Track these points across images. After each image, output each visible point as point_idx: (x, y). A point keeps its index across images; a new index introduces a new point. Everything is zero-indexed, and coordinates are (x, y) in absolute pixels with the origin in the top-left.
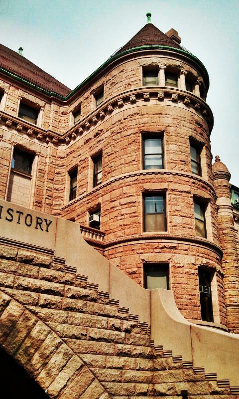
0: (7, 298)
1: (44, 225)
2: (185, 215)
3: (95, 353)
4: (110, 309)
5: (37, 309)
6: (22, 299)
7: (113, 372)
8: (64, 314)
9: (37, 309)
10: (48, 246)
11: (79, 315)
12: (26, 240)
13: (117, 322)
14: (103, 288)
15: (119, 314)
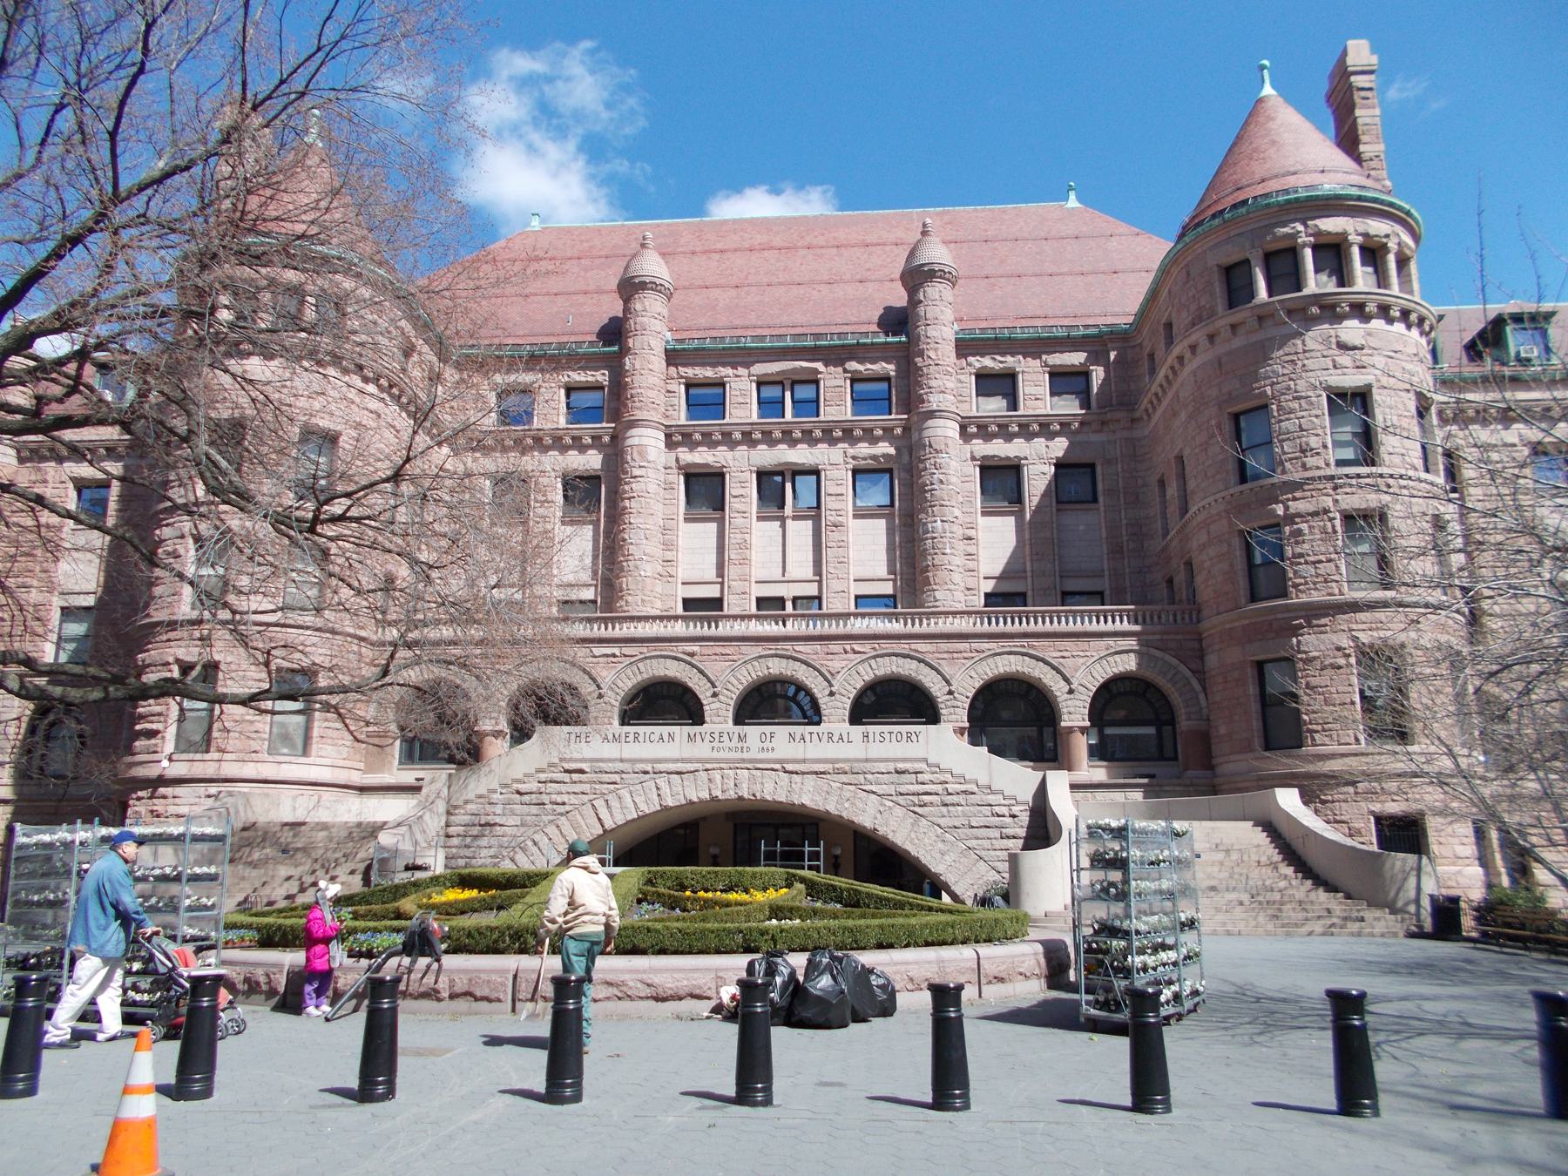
0: (891, 804)
1: (914, 736)
2: (1317, 558)
3: (977, 838)
4: (992, 799)
5: (917, 809)
6: (902, 802)
7: (998, 853)
8: (944, 809)
9: (917, 809)
10: (921, 755)
11: (960, 808)
12: (899, 755)
13: (1004, 810)
14: (983, 781)
15: (1003, 802)
